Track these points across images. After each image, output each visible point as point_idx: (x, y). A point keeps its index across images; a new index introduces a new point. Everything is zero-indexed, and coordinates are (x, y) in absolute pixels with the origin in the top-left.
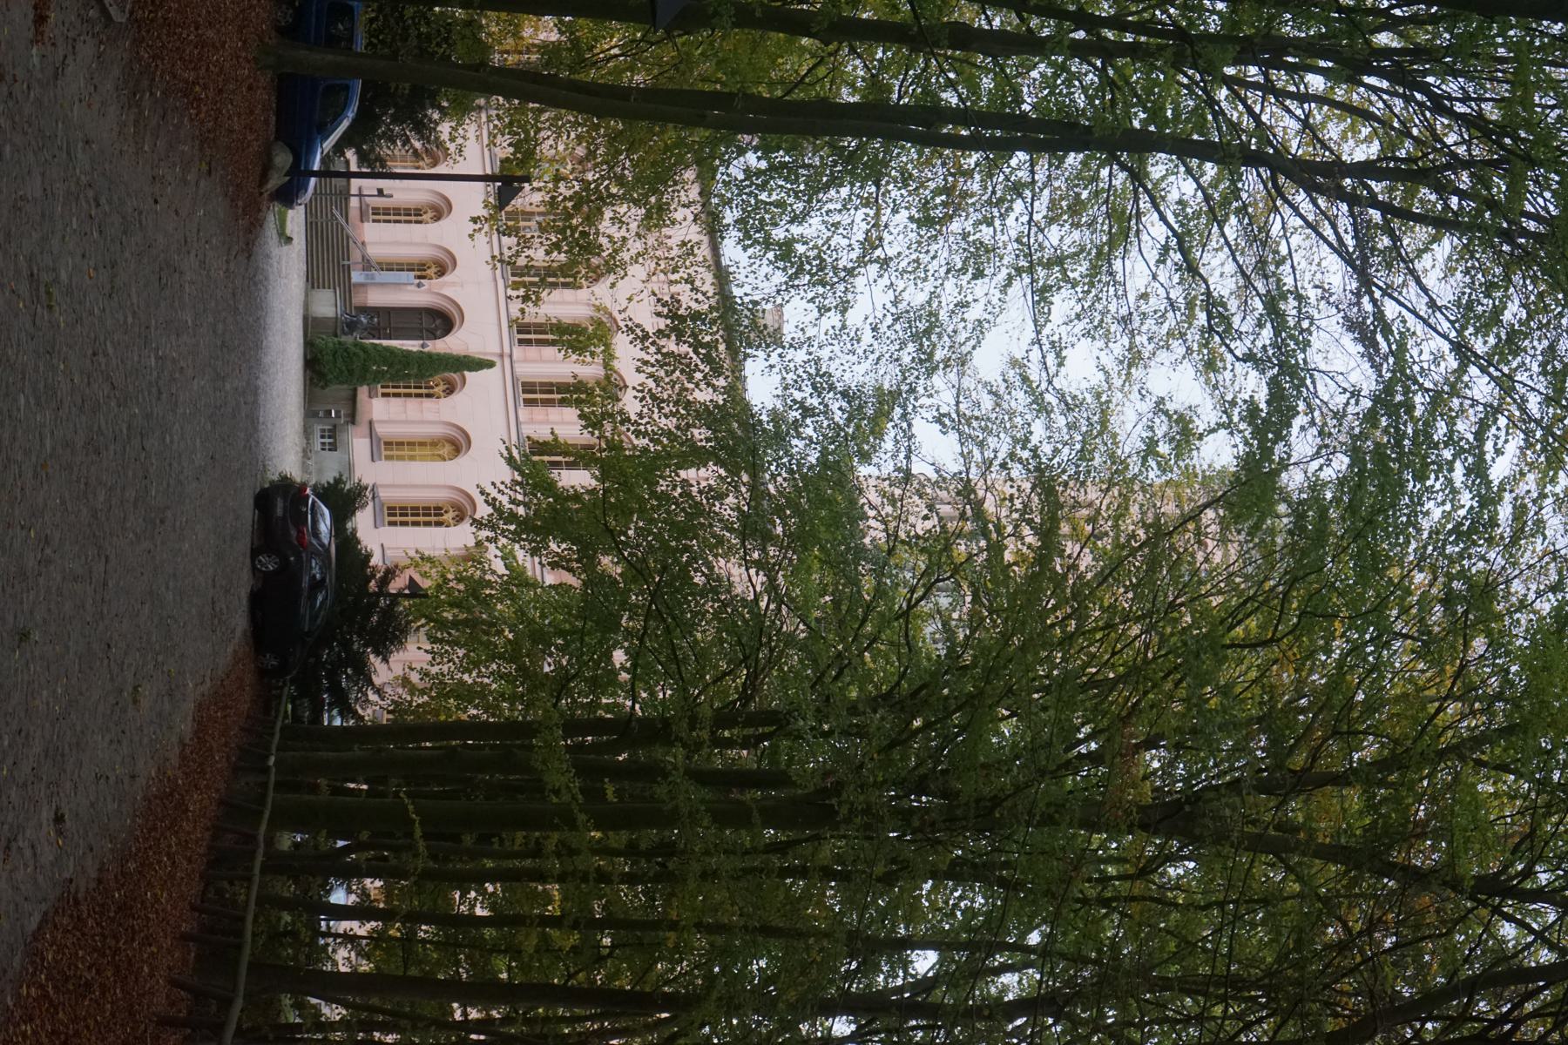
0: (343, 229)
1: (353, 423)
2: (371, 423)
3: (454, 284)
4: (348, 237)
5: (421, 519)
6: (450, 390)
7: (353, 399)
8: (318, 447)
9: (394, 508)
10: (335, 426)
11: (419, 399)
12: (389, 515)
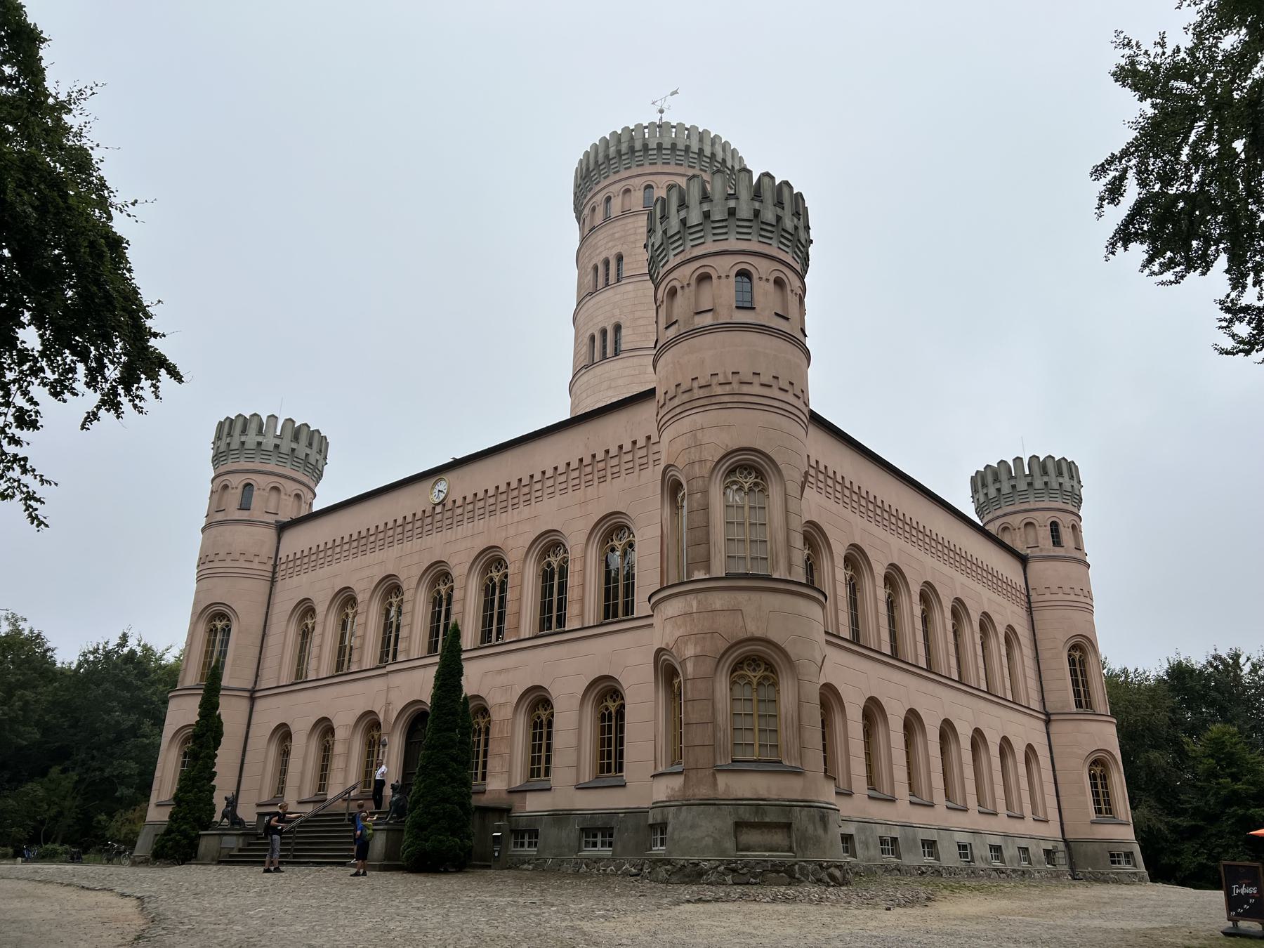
0: (307, 821)
1: (509, 810)
2: (510, 792)
3: (386, 711)
4: (317, 815)
5: (544, 743)
6: (484, 711)
7: (485, 811)
8: (533, 851)
9: (602, 766)
10: (512, 831)
11: (490, 741)
12: (609, 771)
